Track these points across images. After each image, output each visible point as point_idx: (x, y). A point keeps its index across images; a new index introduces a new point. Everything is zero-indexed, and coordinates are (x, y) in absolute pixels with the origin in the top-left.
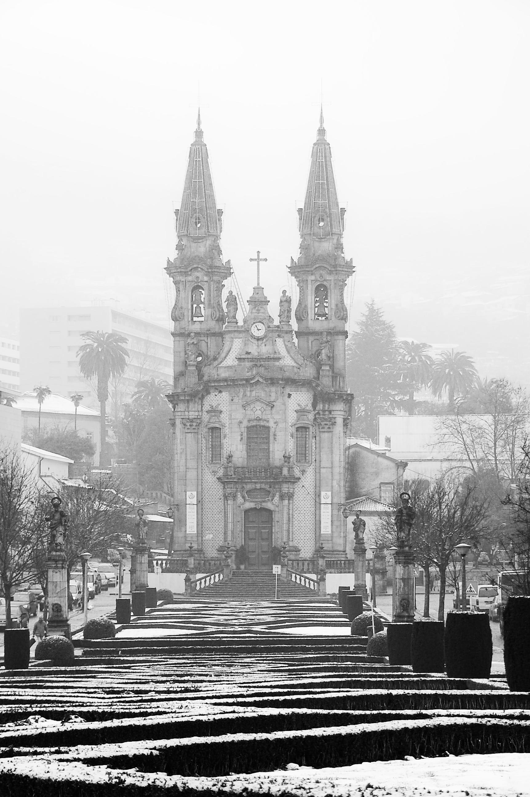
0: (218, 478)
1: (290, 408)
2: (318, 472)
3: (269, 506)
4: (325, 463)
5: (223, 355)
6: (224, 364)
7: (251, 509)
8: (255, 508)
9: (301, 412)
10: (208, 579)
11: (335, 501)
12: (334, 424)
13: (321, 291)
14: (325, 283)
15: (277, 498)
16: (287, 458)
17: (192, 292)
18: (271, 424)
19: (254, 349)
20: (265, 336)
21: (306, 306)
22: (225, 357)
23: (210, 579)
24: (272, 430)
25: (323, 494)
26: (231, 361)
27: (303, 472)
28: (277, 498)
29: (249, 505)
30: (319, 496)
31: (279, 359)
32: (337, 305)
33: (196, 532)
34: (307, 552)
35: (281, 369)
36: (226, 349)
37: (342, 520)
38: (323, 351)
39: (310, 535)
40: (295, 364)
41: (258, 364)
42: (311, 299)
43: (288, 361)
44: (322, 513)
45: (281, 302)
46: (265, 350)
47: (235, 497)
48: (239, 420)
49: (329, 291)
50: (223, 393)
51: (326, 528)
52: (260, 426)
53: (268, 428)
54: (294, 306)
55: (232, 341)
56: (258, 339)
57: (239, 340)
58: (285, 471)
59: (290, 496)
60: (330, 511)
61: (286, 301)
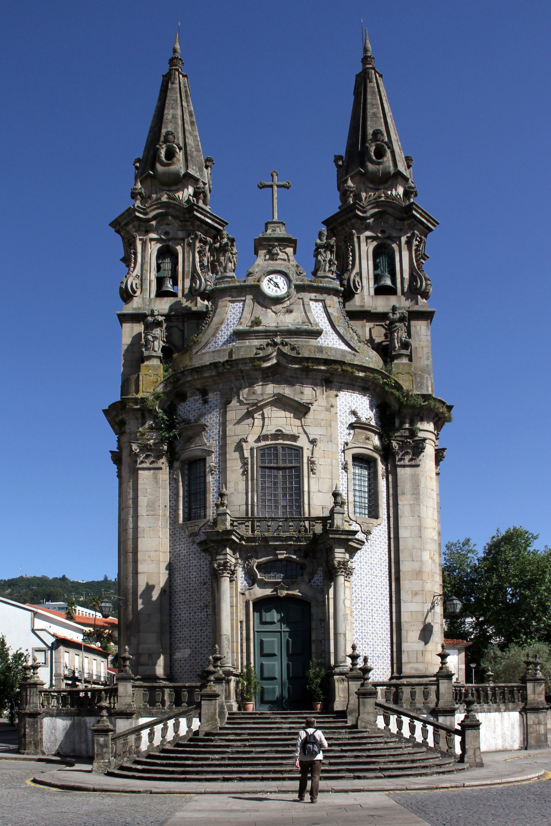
5: (210, 331)
6: (212, 347)
10: (158, 728)
17: (158, 258)
18: (303, 442)
20: (288, 295)
23: (165, 730)
24: (306, 454)
31: (318, 333)
35: (320, 349)
41: (278, 340)
45: (318, 247)
48: (240, 437)
52: (284, 447)
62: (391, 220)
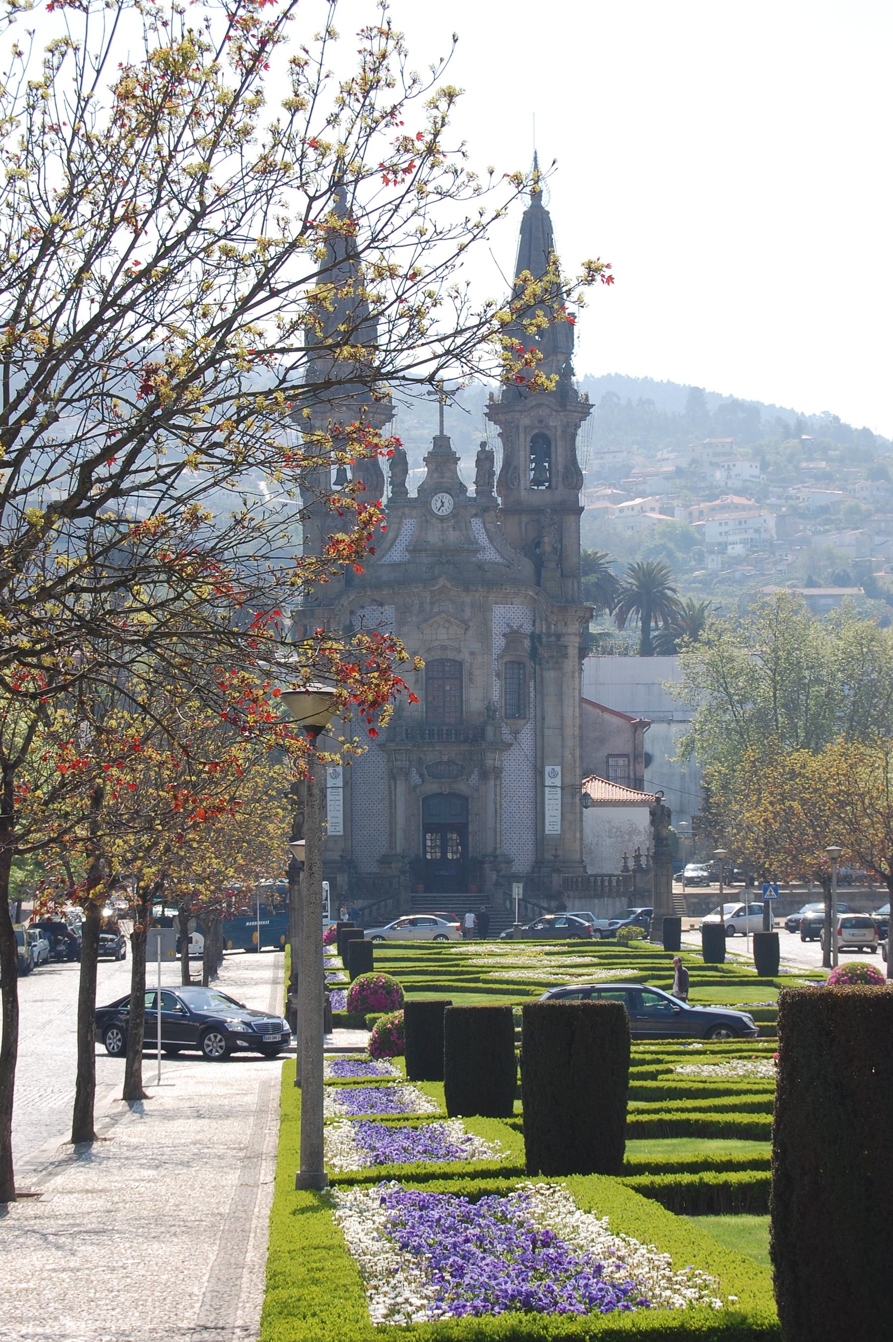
0: (379, 745)
1: (494, 631)
2: (539, 735)
3: (462, 787)
4: (551, 720)
5: (386, 545)
6: (387, 559)
7: (435, 795)
8: (441, 794)
9: (512, 636)
11: (568, 780)
12: (565, 656)
13: (542, 445)
14: (546, 432)
15: (474, 778)
16: (490, 710)
18: (465, 656)
19: (433, 537)
21: (516, 468)
22: (389, 549)
24: (466, 666)
25: (548, 769)
26: (397, 554)
27: (516, 733)
28: (474, 778)
29: (432, 787)
30: (542, 773)
32: (566, 467)
33: (341, 833)
34: (523, 861)
35: (480, 566)
36: (391, 535)
37: (578, 811)
38: (546, 539)
39: (528, 838)
40: (501, 560)
42: (524, 454)
43: (491, 555)
44: (547, 801)
46: (453, 536)
47: (407, 775)
49: (553, 444)
50: (386, 607)
51: (553, 823)
53: (460, 664)
54: (498, 466)
55: (400, 523)
56: (442, 519)
57: (412, 521)
58: (490, 731)
59: (498, 772)
60: (559, 796)
61: (484, 458)
62: (548, 411)
